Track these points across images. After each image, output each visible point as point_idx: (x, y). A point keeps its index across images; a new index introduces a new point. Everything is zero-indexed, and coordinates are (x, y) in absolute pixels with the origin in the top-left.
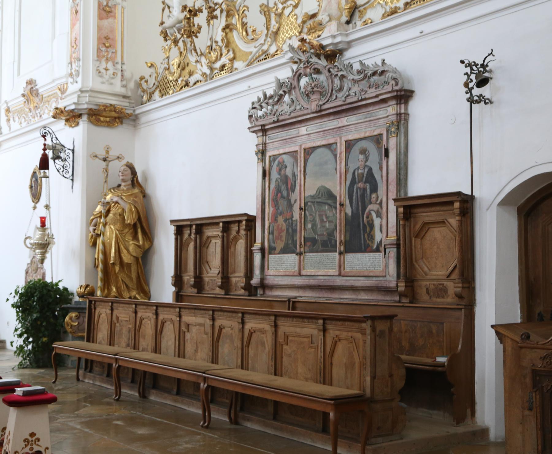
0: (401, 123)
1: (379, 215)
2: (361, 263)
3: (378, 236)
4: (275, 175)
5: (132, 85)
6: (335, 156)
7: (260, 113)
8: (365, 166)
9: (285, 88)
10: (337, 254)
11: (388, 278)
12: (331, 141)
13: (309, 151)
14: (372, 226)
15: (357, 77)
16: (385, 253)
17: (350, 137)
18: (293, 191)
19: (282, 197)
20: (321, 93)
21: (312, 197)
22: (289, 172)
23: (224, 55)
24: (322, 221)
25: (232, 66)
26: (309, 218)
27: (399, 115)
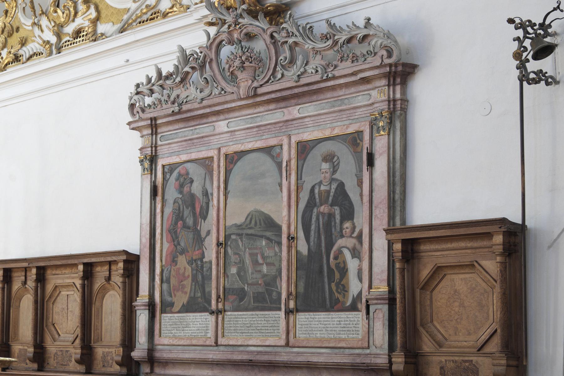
0: (397, 115)
1: (356, 253)
3: (355, 287)
4: (172, 194)
6: (279, 165)
7: (148, 100)
8: (332, 180)
9: (193, 64)
10: (282, 314)
11: (373, 350)
12: (273, 142)
13: (232, 159)
14: (344, 271)
15: (320, 45)
16: (368, 313)
17: (308, 136)
18: (204, 217)
19: (185, 226)
21: (239, 227)
22: (196, 189)
23: (80, 13)
25: (95, 31)
26: (233, 258)
27: (392, 102)
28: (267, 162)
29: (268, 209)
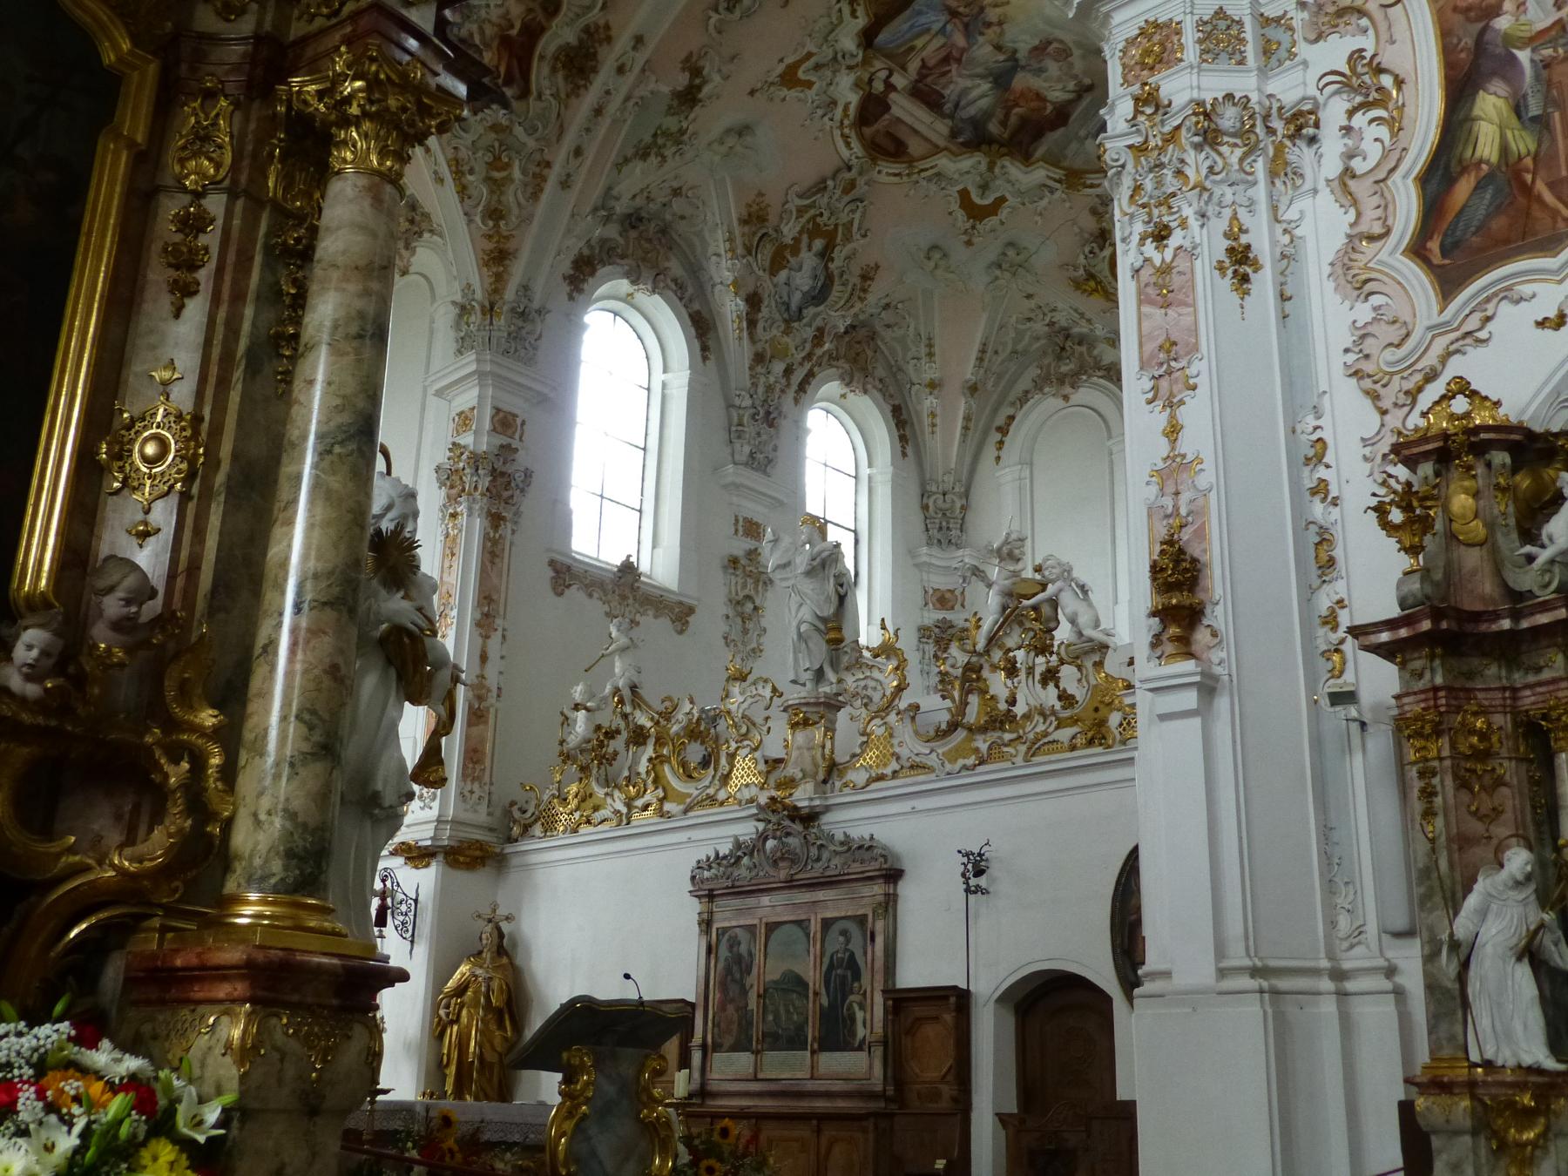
0: (889, 904)
1: (862, 1007)
2: (837, 1063)
3: (861, 1032)
4: (724, 952)
5: (498, 812)
7: (706, 874)
8: (846, 950)
13: (771, 927)
14: (853, 1019)
18: (749, 973)
20: (793, 861)
21: (775, 982)
22: (743, 949)
24: (788, 1011)
27: (887, 895)
28: (797, 932)
29: (798, 969)
